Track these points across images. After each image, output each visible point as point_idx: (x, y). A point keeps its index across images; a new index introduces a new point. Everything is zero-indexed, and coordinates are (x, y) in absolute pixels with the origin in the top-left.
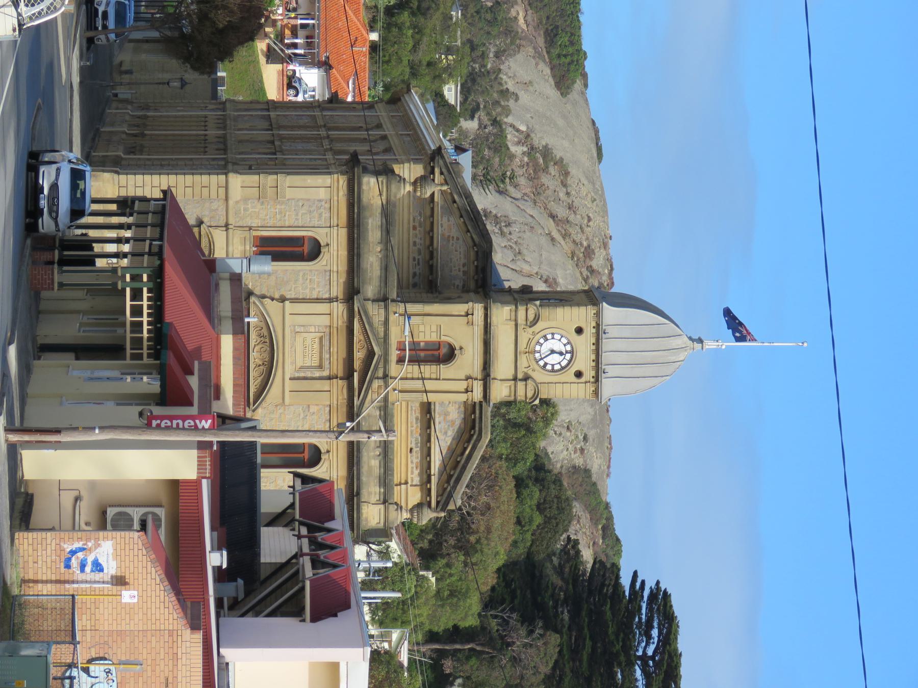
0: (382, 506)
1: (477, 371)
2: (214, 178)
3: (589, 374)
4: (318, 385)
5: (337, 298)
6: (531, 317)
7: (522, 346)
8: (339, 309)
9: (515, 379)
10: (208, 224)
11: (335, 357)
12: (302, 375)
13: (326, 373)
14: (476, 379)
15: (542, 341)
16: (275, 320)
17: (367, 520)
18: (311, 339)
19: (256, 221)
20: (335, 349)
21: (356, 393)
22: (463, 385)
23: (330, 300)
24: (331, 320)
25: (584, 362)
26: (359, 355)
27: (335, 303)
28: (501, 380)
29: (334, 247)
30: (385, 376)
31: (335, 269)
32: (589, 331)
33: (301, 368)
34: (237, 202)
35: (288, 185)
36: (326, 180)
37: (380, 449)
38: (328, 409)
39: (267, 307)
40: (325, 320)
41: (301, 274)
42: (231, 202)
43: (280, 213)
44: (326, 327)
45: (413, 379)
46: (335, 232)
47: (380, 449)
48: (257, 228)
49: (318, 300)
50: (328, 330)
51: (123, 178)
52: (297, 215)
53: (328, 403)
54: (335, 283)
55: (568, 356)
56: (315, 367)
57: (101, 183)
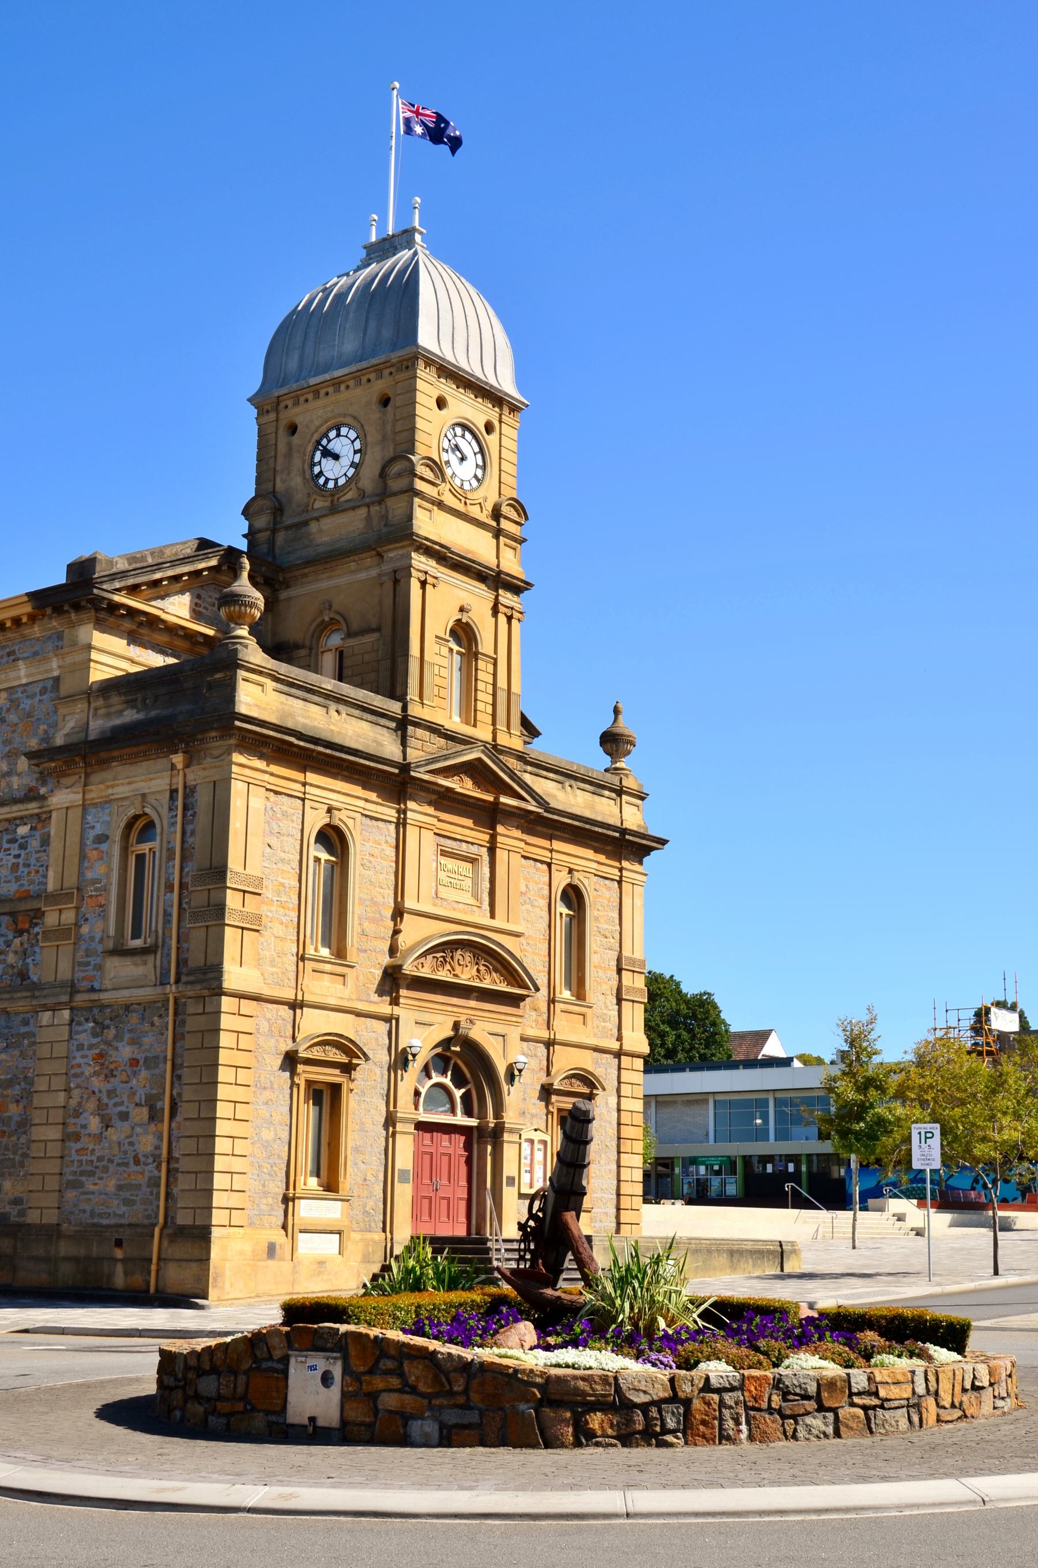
0: (624, 797)
2: (226, 1022)
5: (398, 811)
6: (428, 474)
7: (459, 506)
8: (417, 811)
9: (498, 533)
10: (290, 1041)
14: (497, 597)
16: (438, 932)
17: (639, 826)
20: (459, 830)
23: (401, 824)
25: (479, 412)
27: (409, 814)
28: (498, 557)
29: (336, 800)
31: (362, 803)
32: (448, 389)
33: (476, 895)
35: (240, 869)
36: (237, 788)
37: (567, 784)
39: (410, 942)
40: (428, 837)
42: (267, 992)
48: (300, 942)
49: (400, 847)
51: (218, 1217)
52: (283, 860)
56: (476, 872)
57: (228, 1265)
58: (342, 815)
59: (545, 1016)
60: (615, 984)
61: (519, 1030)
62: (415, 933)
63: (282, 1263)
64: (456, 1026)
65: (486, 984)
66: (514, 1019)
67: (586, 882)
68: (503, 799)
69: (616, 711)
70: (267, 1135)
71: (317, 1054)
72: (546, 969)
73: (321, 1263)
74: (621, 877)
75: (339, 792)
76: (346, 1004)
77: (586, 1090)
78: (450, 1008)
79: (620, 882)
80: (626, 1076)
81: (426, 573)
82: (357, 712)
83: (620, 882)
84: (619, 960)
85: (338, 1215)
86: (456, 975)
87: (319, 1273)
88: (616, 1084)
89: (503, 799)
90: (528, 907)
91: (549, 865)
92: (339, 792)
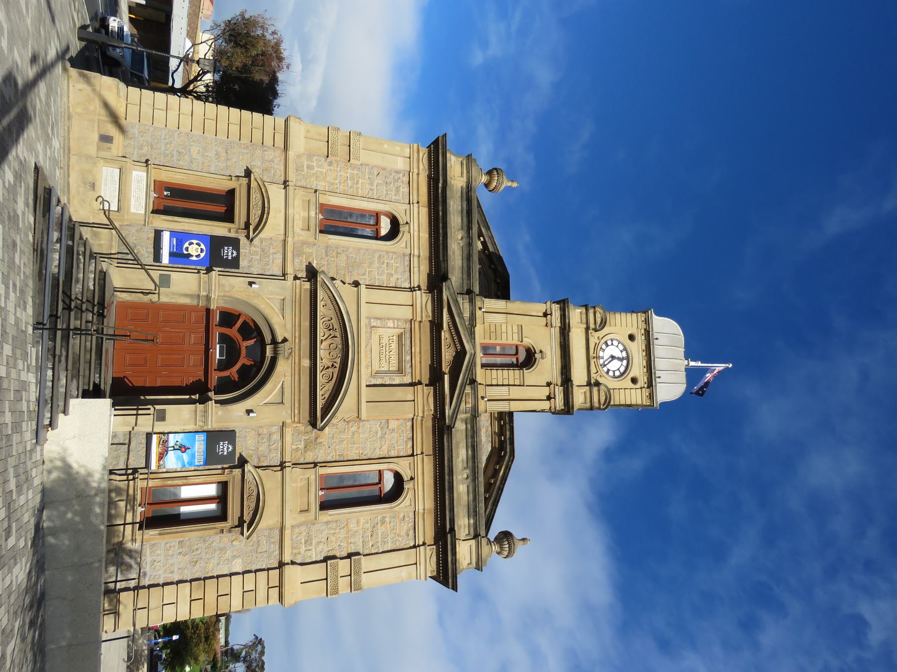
0: (473, 542)
1: (557, 378)
3: (643, 380)
4: (400, 393)
5: (419, 287)
11: (418, 359)
12: (379, 382)
13: (407, 380)
15: (604, 347)
16: (348, 306)
18: (389, 333)
19: (323, 183)
20: (418, 349)
21: (448, 400)
22: (545, 392)
24: (414, 312)
25: (638, 370)
26: (447, 355)
29: (414, 226)
30: (473, 382)
31: (416, 253)
34: (299, 156)
37: (468, 471)
38: (410, 424)
40: (407, 313)
41: (377, 255)
43: (352, 178)
44: (406, 321)
45: (497, 385)
46: (416, 209)
47: (468, 471)
49: (396, 288)
50: (408, 326)
52: (372, 184)
53: (412, 416)
54: (416, 269)
55: (625, 362)
58: (406, 237)
59: (301, 461)
60: (338, 555)
61: (289, 421)
62: (346, 293)
63: (95, 145)
64: (285, 340)
65: (319, 393)
66: (296, 412)
67: (407, 502)
68: (446, 377)
69: (524, 539)
70: (195, 150)
71: (255, 196)
72: (338, 459)
73: (93, 186)
74: (419, 546)
75: (419, 231)
76: (290, 225)
77: (247, 518)
78: (297, 334)
79: (414, 547)
80: (262, 576)
81: (551, 314)
82: (465, 252)
83: (414, 547)
84: (358, 554)
85: (133, 210)
86: (322, 341)
87: (85, 183)
88: (254, 568)
89: (446, 377)
90: (379, 434)
91: (412, 455)
92: (419, 231)
